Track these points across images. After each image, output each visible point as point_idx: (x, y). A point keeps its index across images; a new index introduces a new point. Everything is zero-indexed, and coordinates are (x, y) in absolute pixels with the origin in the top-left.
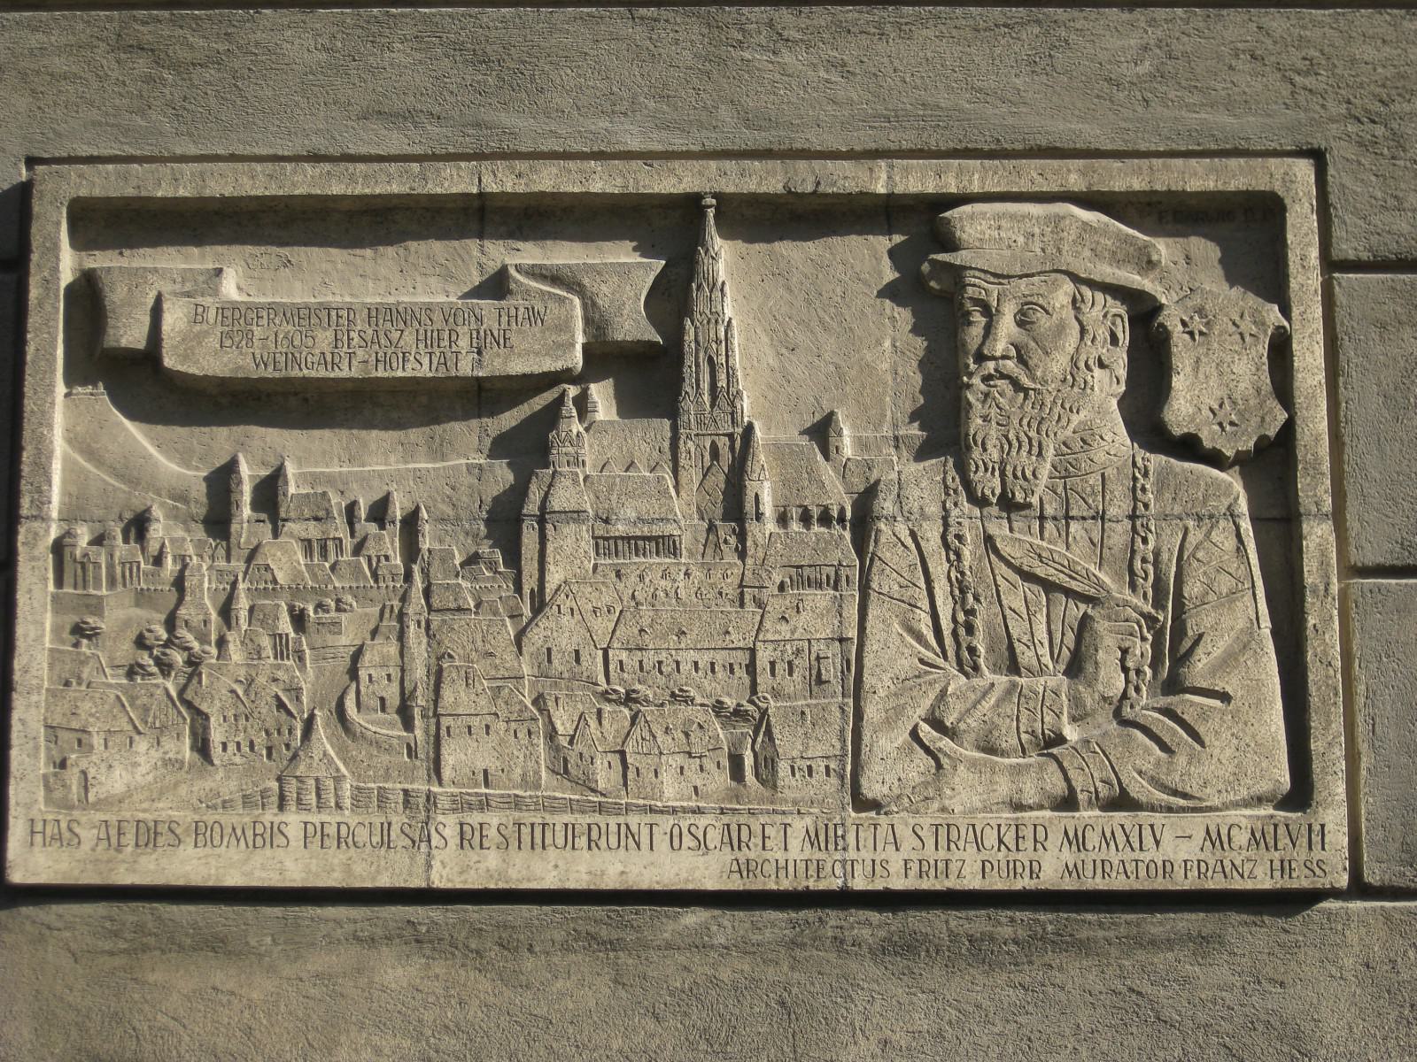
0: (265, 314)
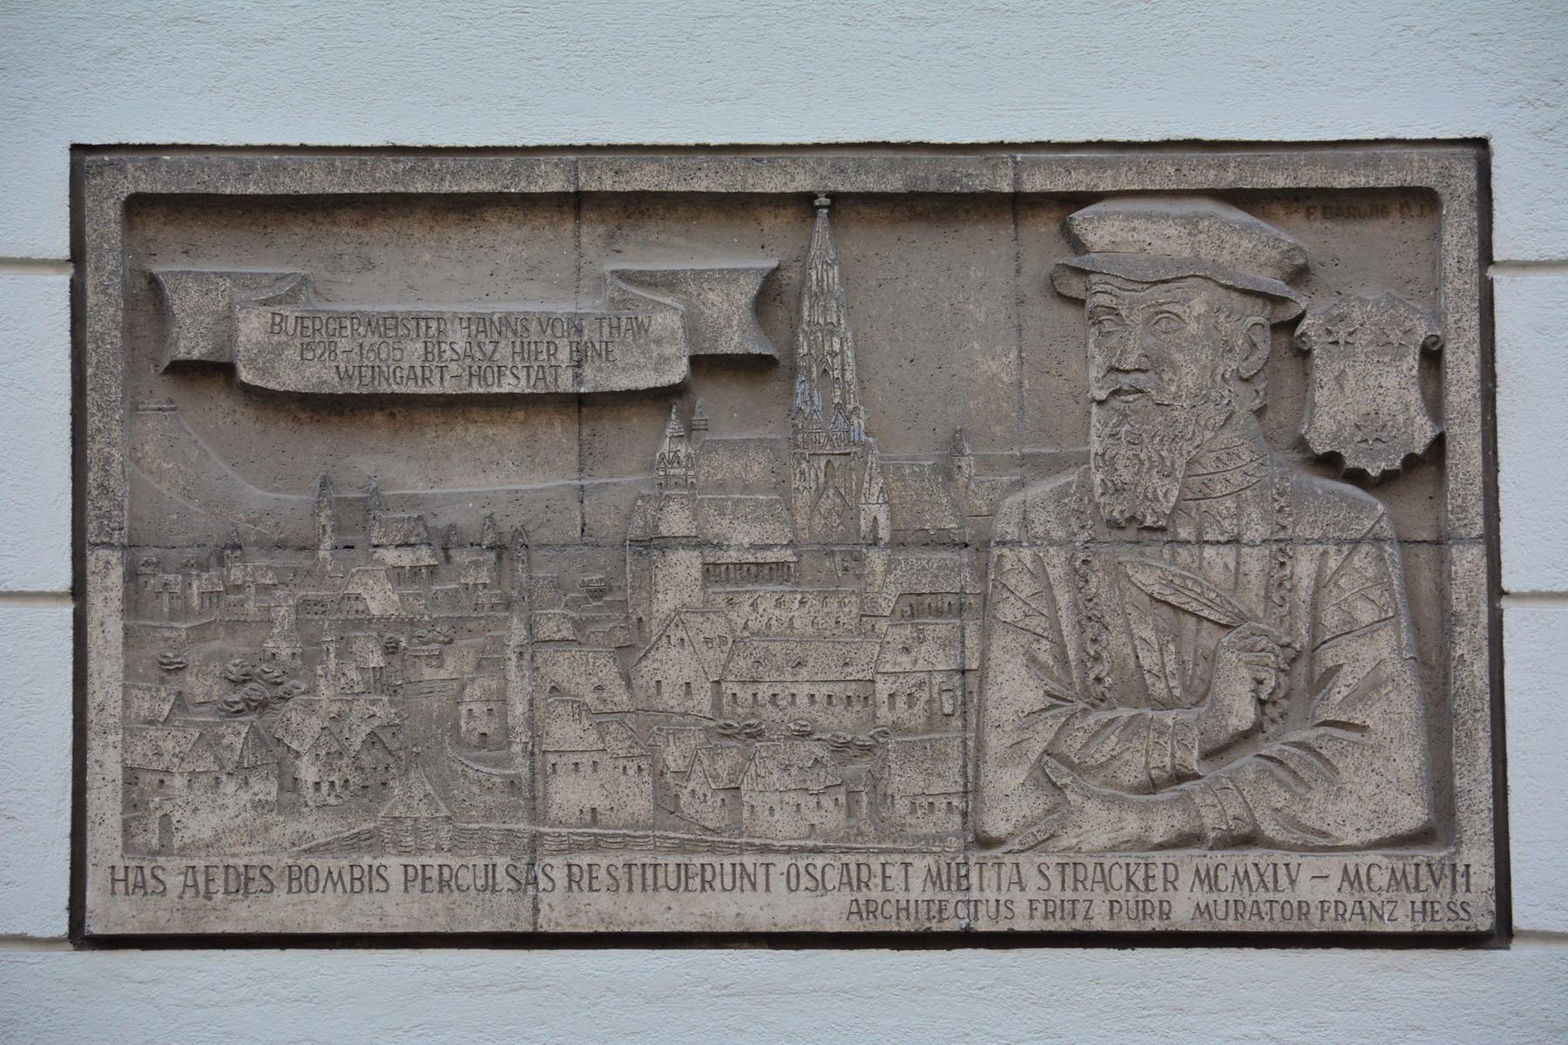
0: (348, 323)
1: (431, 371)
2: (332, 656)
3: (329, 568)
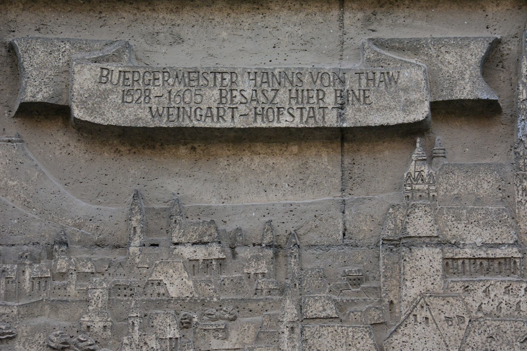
0: (160, 76)
1: (225, 111)
2: (136, 328)
3: (137, 260)
